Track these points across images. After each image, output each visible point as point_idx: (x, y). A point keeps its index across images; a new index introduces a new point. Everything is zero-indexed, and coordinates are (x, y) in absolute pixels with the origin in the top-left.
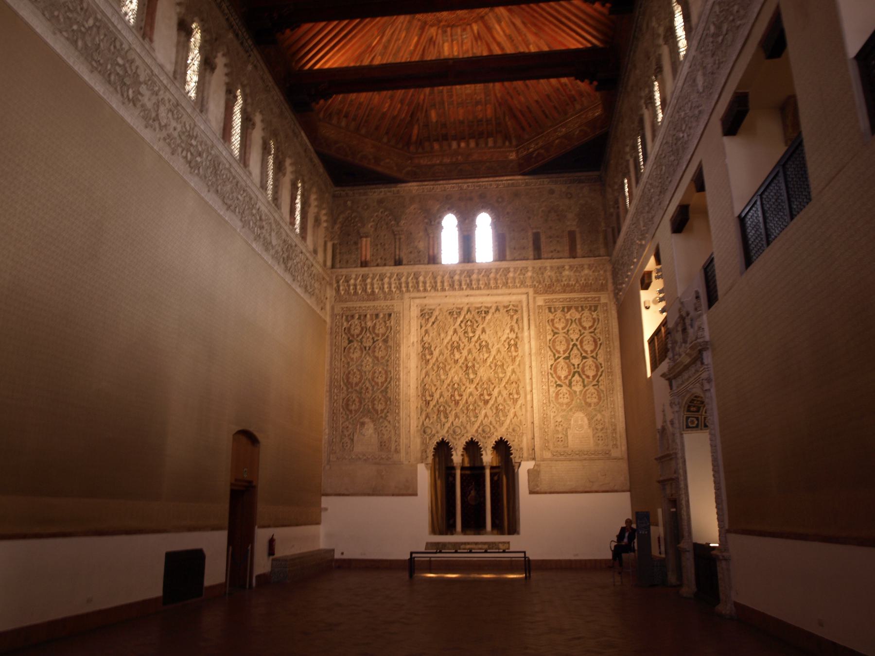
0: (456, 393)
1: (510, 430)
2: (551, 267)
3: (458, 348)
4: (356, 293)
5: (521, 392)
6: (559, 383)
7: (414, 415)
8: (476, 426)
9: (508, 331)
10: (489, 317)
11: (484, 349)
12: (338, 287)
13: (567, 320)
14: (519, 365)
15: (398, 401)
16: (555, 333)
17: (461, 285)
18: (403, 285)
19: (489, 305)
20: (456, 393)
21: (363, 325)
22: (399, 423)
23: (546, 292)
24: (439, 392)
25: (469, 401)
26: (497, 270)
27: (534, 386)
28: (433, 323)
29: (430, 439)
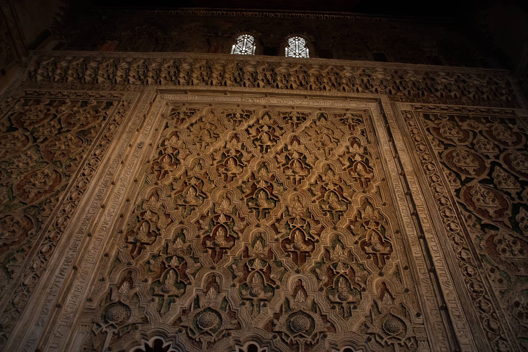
0: (220, 232)
1: (376, 329)
2: (416, 72)
3: (238, 159)
4: (64, 79)
5: (393, 242)
6: (485, 221)
7: (90, 268)
8: (269, 312)
9: (348, 144)
10: (308, 123)
11: (296, 165)
12: (36, 71)
13: (466, 132)
14: (379, 192)
15: (59, 229)
16: (447, 146)
17: (255, 79)
18: (150, 74)
19: (306, 111)
20: (220, 232)
21: (53, 111)
22: (36, 277)
23: (412, 101)
24: (176, 226)
25: (252, 253)
26: (321, 67)
27: (426, 225)
28: (192, 125)
29: (117, 337)
